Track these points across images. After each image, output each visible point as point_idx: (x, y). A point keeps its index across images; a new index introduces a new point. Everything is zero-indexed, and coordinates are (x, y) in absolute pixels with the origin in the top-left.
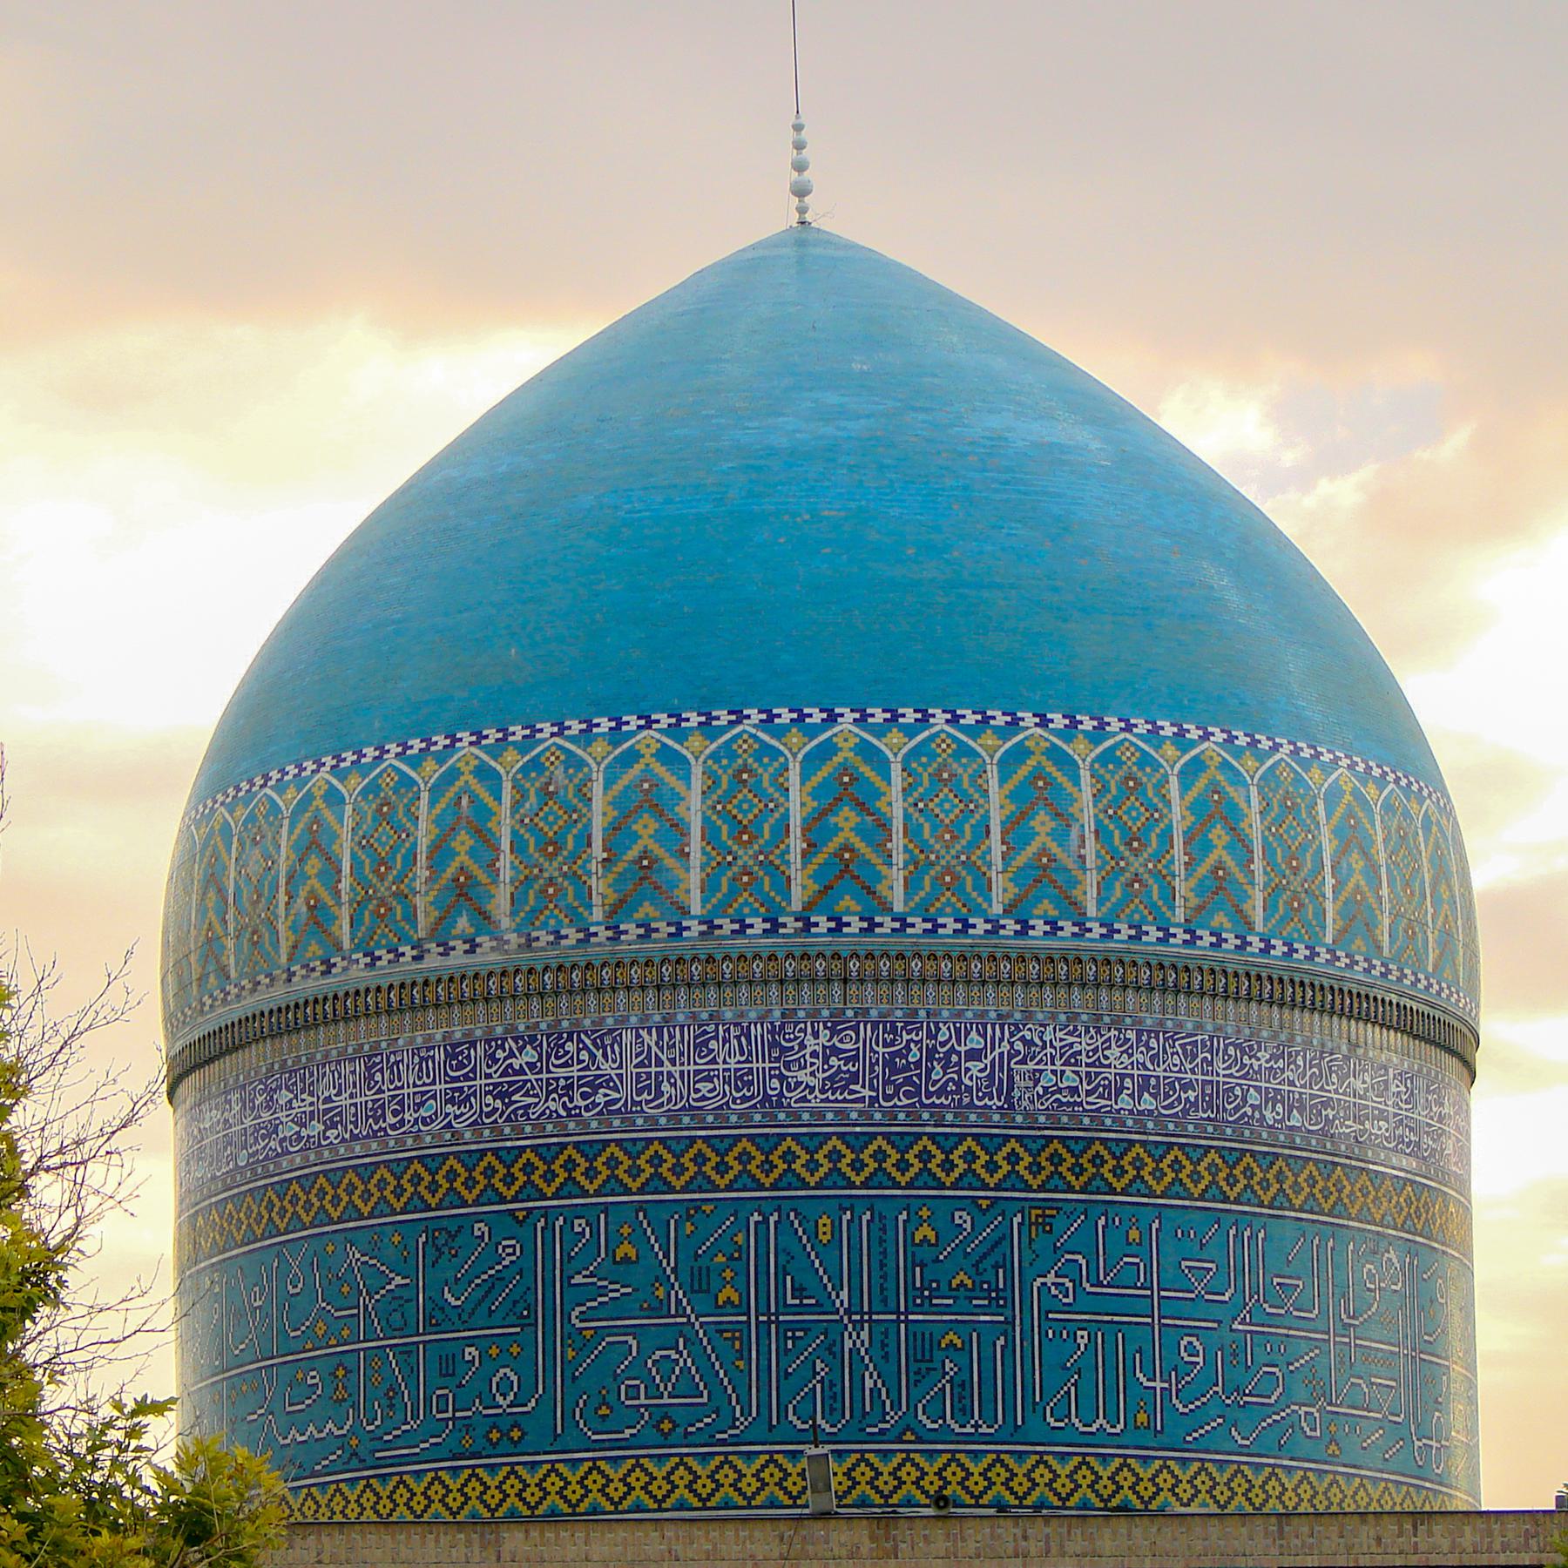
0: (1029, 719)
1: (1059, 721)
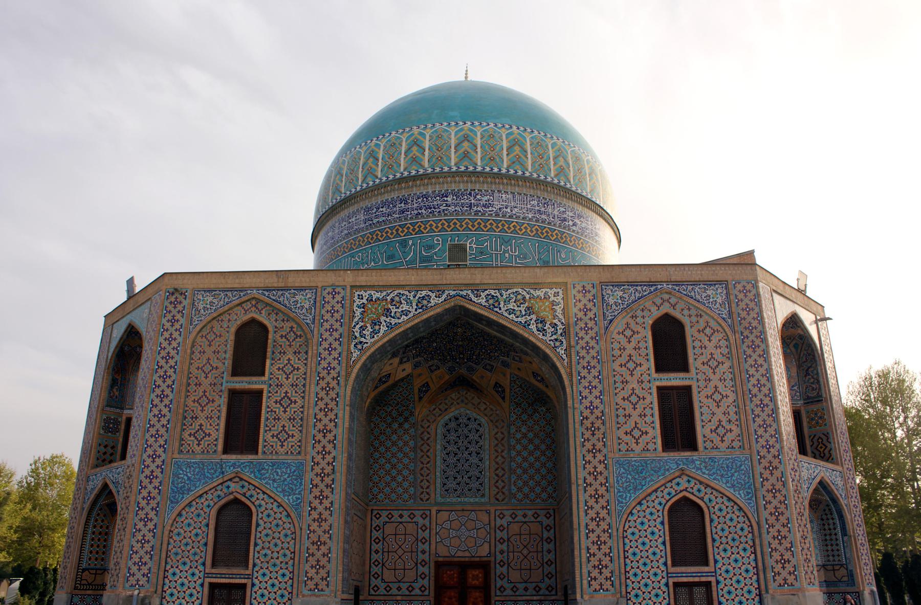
0: (514, 128)
1: (522, 129)
